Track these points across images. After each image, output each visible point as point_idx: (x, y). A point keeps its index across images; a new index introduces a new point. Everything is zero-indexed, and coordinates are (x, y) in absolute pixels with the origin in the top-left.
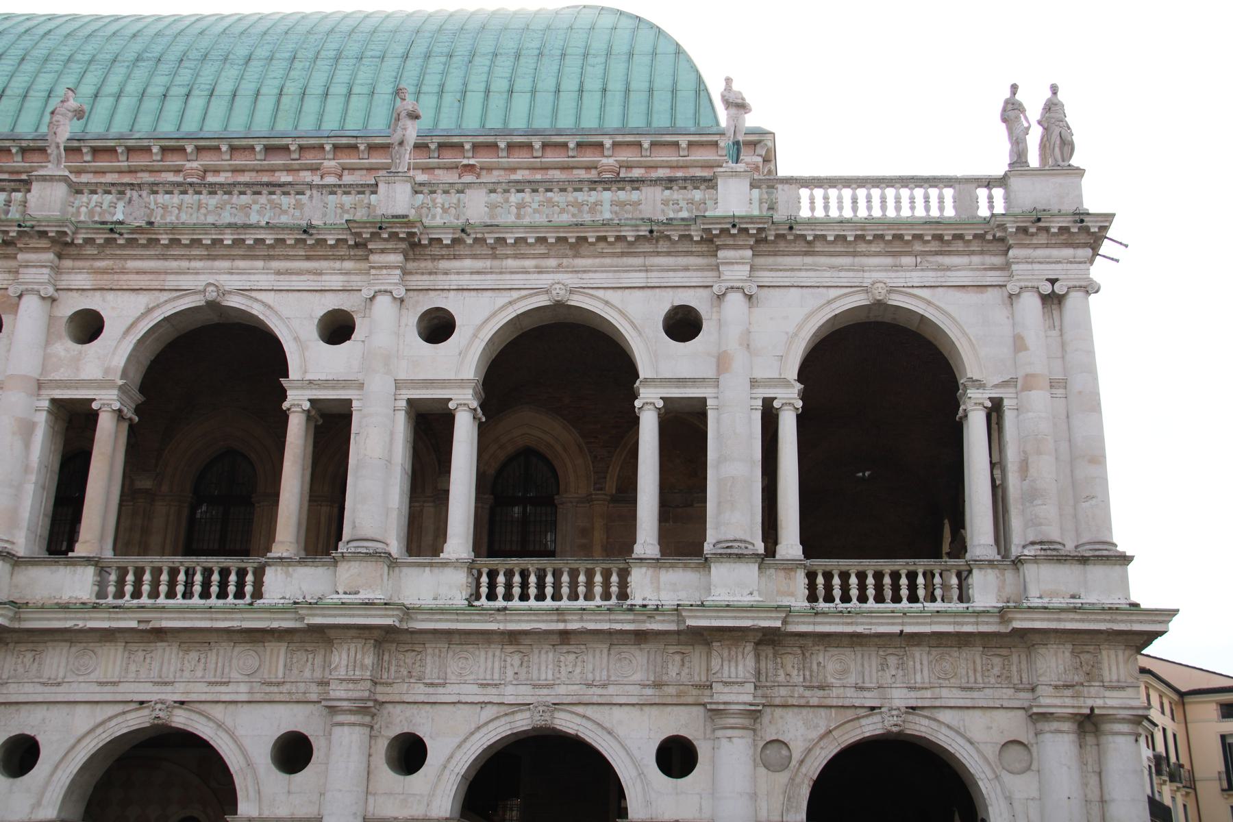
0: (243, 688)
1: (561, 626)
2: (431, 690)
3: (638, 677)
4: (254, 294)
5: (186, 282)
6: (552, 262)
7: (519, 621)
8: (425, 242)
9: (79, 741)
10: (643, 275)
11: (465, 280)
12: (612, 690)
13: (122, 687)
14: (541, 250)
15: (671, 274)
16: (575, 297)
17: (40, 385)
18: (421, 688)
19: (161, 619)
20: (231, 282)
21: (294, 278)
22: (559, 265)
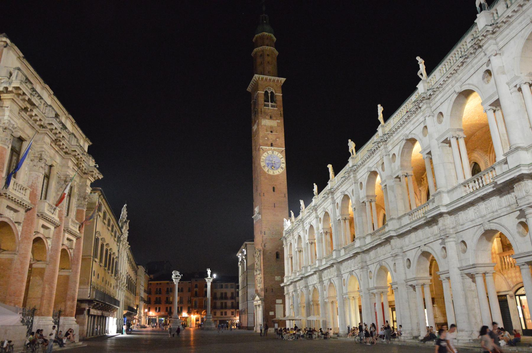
0: (432, 238)
1: (476, 197)
2: (462, 226)
3: (504, 205)
4: (412, 132)
5: (402, 138)
6: (454, 82)
7: (467, 199)
8: (428, 97)
9: (414, 258)
10: (473, 69)
11: (442, 100)
12: (499, 212)
13: (417, 243)
14: (450, 80)
15: (479, 63)
16: (462, 88)
17: (391, 176)
18: (460, 227)
19: (412, 225)
20: (407, 132)
21: (416, 123)
22: (456, 81)
